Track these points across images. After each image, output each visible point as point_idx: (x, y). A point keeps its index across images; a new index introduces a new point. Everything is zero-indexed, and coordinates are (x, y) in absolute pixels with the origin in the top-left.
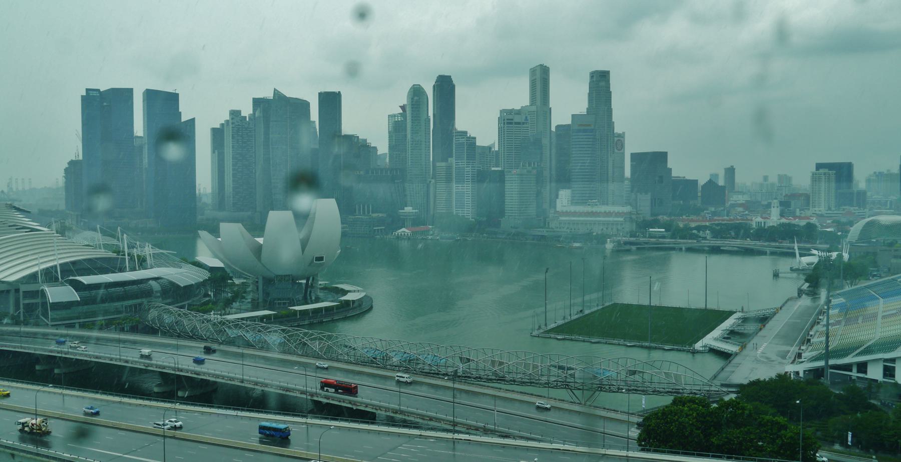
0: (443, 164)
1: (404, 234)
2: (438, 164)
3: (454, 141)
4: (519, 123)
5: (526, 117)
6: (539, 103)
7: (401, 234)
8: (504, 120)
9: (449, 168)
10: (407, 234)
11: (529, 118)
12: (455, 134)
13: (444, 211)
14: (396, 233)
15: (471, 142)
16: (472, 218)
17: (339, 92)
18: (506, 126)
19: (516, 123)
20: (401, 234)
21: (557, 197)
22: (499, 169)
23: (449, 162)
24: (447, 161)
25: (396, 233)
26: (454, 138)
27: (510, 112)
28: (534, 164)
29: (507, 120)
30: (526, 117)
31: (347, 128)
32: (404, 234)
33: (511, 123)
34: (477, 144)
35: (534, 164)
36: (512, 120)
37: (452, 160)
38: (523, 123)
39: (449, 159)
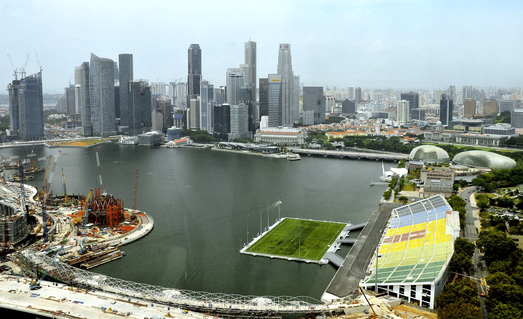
0: (194, 100)
1: (172, 145)
2: (191, 100)
3: (201, 87)
4: (239, 77)
5: (243, 73)
6: (250, 62)
7: (170, 145)
8: (230, 75)
9: (197, 103)
10: (174, 145)
11: (244, 73)
12: (201, 83)
13: (195, 128)
14: (167, 144)
15: (211, 90)
16: (211, 132)
17: (132, 54)
18: (231, 78)
19: (237, 77)
20: (170, 145)
21: (260, 120)
22: (227, 104)
23: (198, 98)
24: (196, 98)
25: (167, 144)
26: (201, 85)
27: (234, 70)
28: (247, 101)
29: (232, 75)
30: (243, 73)
31: (136, 77)
32: (172, 145)
33: (234, 77)
34: (214, 88)
35: (247, 101)
36: (234, 75)
37: (199, 98)
38: (241, 77)
39: (198, 97)
